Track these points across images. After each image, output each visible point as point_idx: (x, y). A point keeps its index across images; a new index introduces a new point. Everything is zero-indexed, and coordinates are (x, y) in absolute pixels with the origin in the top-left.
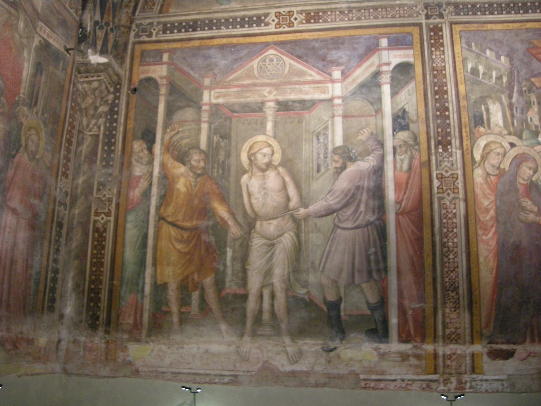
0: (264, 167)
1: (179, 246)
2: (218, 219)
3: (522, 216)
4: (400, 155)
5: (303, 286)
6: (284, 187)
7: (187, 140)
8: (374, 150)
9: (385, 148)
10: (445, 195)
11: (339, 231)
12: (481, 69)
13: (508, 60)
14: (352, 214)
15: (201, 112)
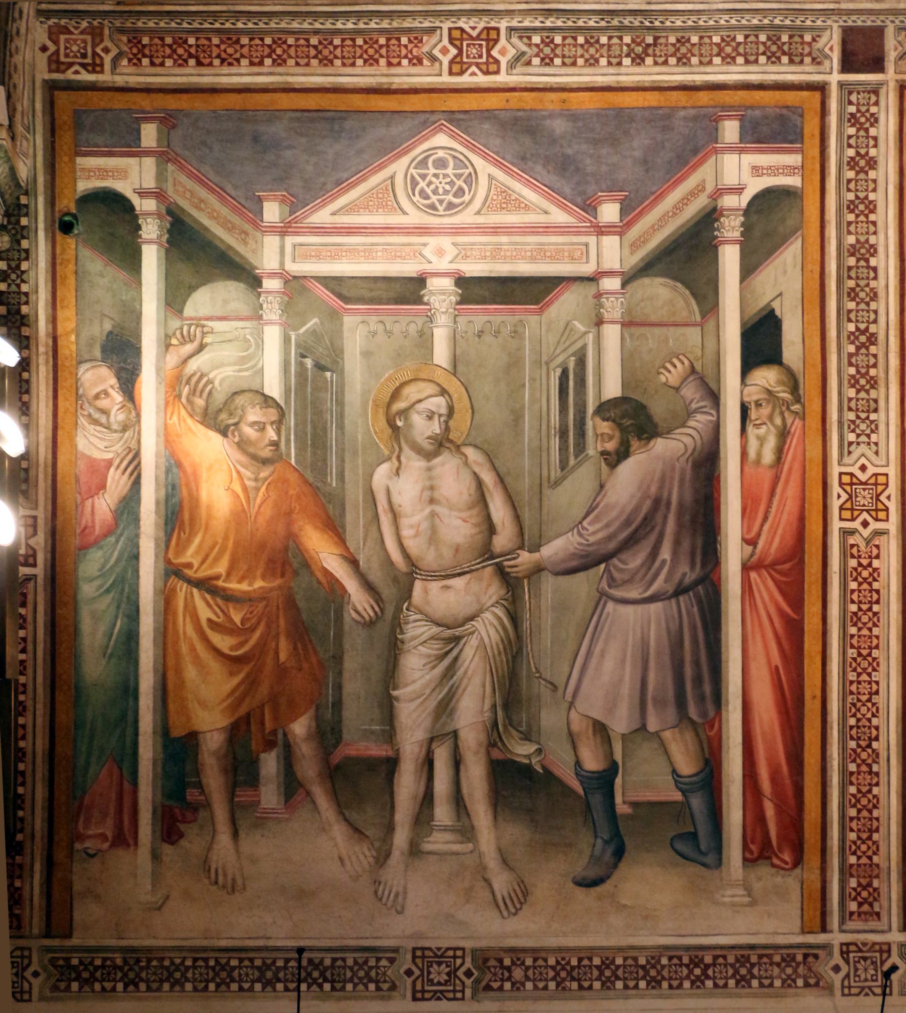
0: (427, 446)
1: (223, 642)
2: (319, 575)
4: (757, 426)
5: (527, 737)
6: (481, 498)
7: (229, 371)
8: (696, 411)
9: (721, 407)
10: (857, 524)
11: (610, 606)
14: (643, 565)
15: (259, 294)
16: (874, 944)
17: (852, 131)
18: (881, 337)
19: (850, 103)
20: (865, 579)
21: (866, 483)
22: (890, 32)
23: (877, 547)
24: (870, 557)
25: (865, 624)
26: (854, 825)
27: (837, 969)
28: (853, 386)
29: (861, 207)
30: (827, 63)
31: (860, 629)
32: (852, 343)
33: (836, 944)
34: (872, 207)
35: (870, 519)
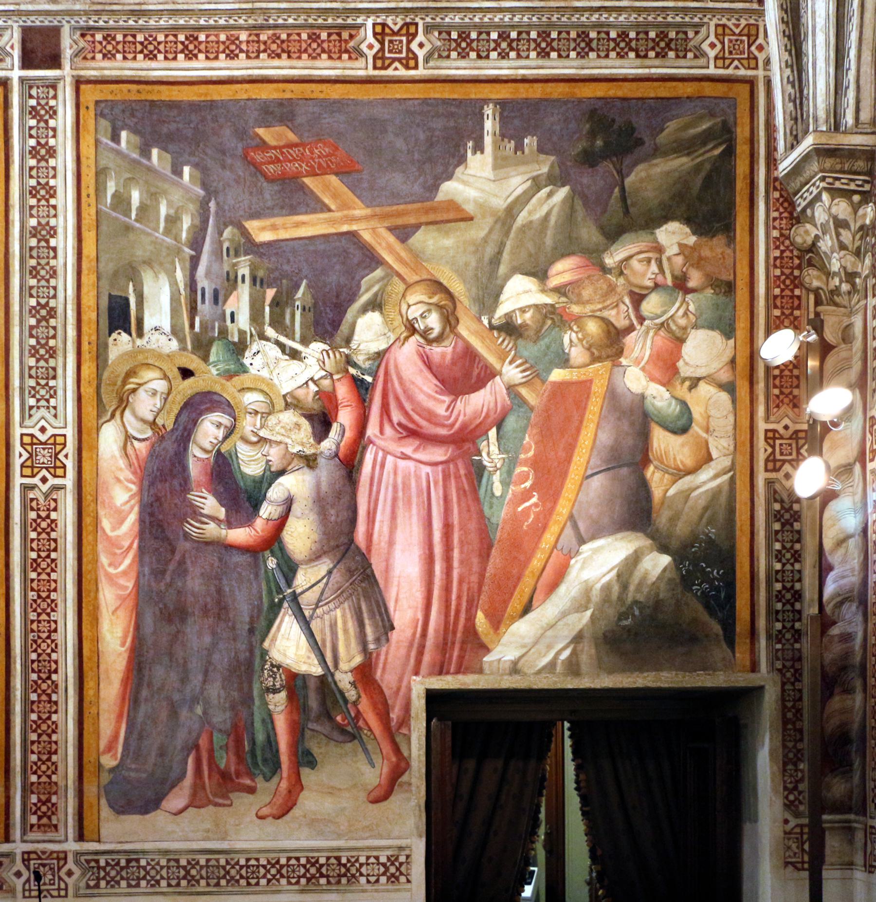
3: (192, 528)
10: (36, 480)
12: (136, 196)
13: (198, 174)
16: (52, 852)
17: (33, 122)
18: (60, 310)
19: (31, 97)
20: (44, 529)
21: (45, 443)
22: (66, 31)
23: (55, 500)
24: (48, 510)
25: (44, 569)
26: (35, 747)
27: (18, 874)
28: (33, 356)
29: (43, 192)
30: (8, 60)
31: (39, 574)
32: (34, 316)
33: (18, 852)
34: (52, 192)
35: (48, 476)
